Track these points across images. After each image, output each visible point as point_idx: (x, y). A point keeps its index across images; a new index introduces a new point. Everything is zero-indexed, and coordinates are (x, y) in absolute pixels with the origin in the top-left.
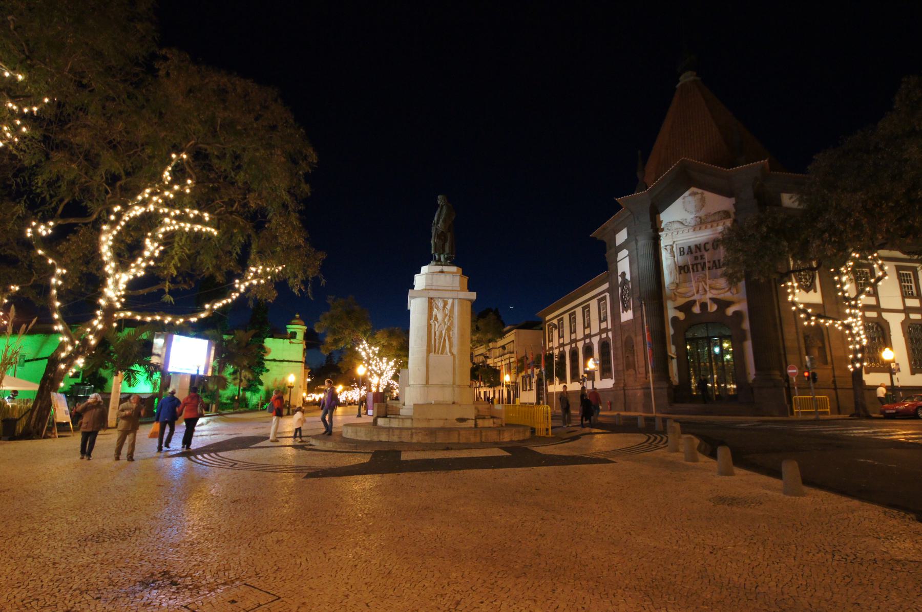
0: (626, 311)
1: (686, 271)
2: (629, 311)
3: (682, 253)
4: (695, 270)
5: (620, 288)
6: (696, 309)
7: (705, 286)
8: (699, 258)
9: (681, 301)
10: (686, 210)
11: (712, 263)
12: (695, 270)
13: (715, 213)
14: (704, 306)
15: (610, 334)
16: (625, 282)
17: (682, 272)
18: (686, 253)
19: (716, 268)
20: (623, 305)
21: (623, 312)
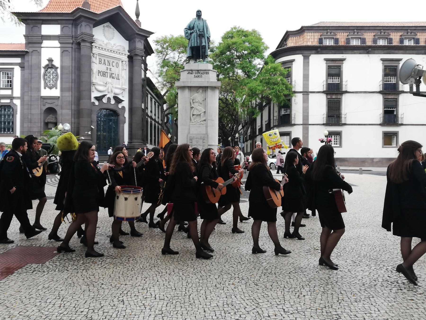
0: (51, 88)
1: (102, 75)
2: (54, 89)
3: (100, 63)
4: (106, 76)
5: (43, 71)
6: (105, 100)
7: (112, 88)
8: (109, 69)
9: (99, 95)
10: (104, 36)
11: (115, 74)
12: (106, 76)
13: (120, 46)
14: (109, 99)
15: (17, 102)
16: (50, 66)
17: (99, 74)
18: (102, 63)
19: (117, 79)
20: (45, 83)
21: (45, 88)
